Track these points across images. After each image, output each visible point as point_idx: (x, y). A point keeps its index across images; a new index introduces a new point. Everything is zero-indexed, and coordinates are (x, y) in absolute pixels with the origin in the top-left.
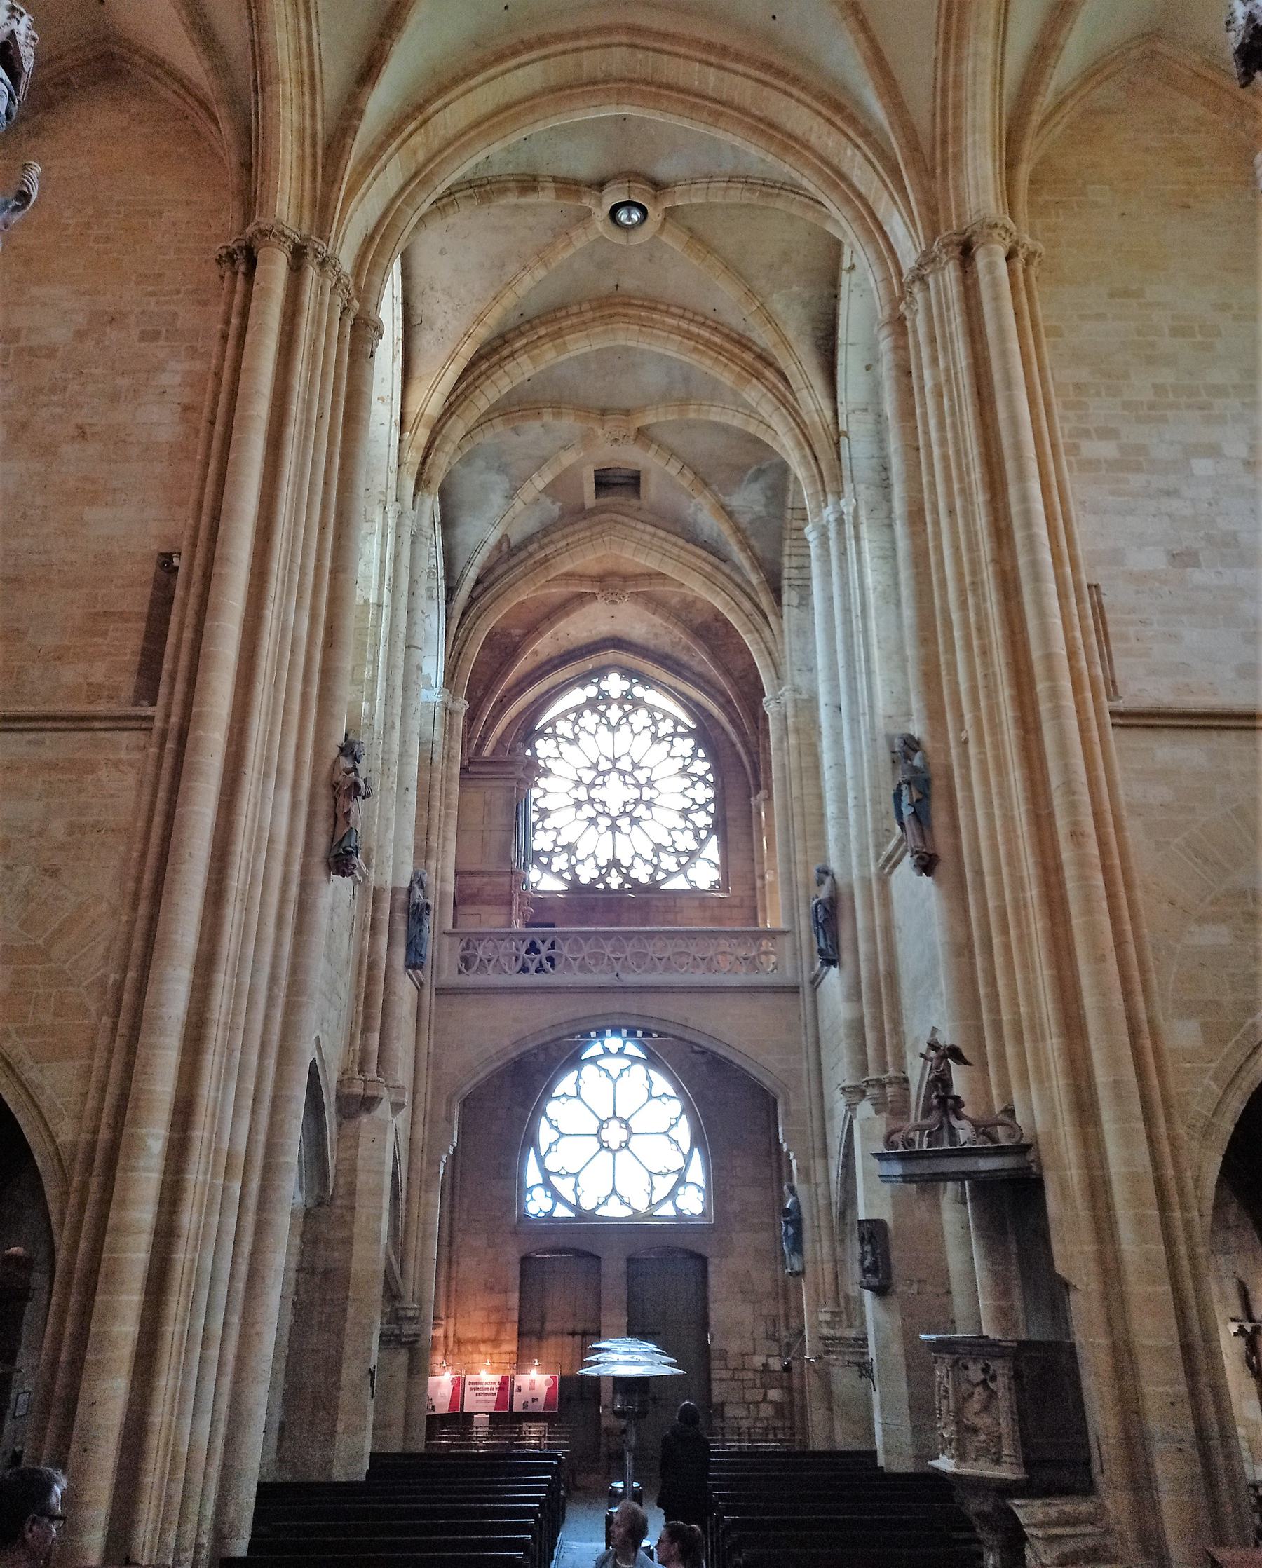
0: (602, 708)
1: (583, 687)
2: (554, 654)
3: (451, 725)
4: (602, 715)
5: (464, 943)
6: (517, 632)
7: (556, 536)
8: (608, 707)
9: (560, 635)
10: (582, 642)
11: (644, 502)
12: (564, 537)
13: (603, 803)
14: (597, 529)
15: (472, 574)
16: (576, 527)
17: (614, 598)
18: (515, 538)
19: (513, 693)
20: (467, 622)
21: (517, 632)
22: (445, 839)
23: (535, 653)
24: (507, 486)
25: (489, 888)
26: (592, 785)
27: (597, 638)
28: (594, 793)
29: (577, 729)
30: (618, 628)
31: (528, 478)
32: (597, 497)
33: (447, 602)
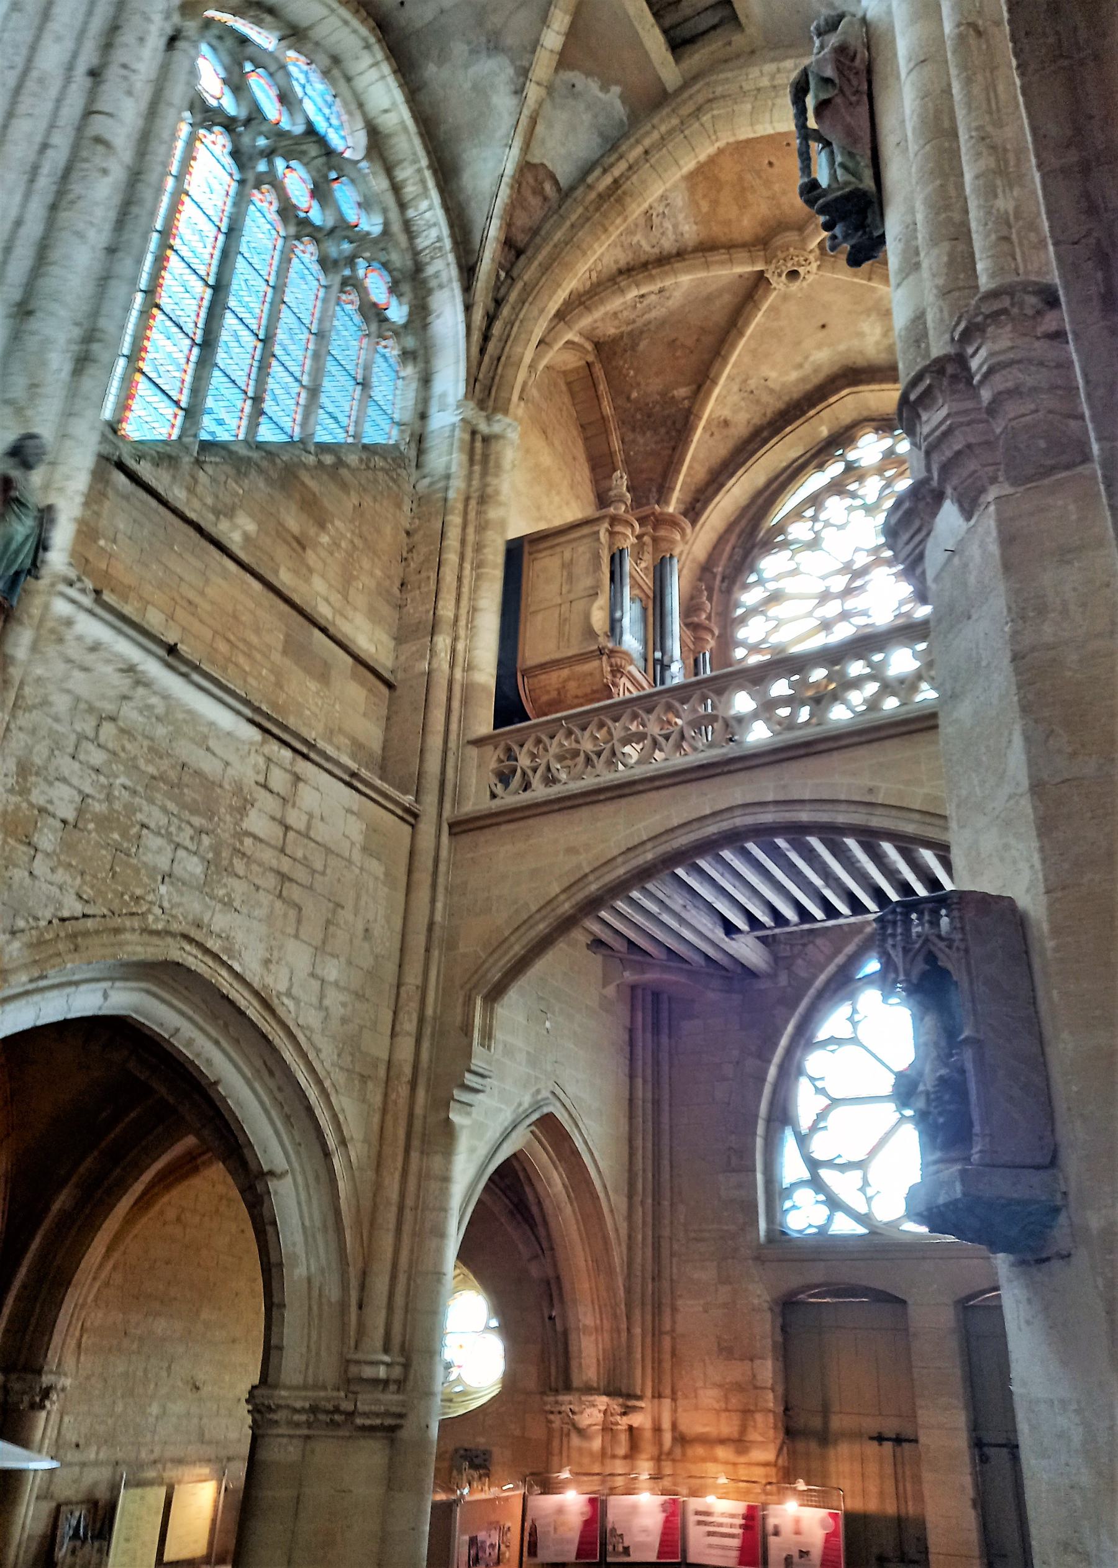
0: (852, 487)
1: (821, 467)
2: (757, 421)
3: (485, 458)
4: (853, 495)
5: (500, 753)
6: (681, 392)
7: (624, 148)
8: (861, 479)
9: (752, 383)
10: (795, 396)
11: (751, 30)
12: (638, 142)
13: (864, 613)
14: (685, 111)
15: (494, 230)
16: (655, 121)
17: (790, 267)
18: (564, 172)
19: (710, 490)
20: (506, 311)
21: (681, 392)
22: (474, 610)
23: (726, 423)
24: (511, 71)
25: (572, 685)
26: (848, 592)
27: (816, 380)
28: (851, 604)
29: (818, 526)
30: (842, 347)
31: (535, 45)
32: (677, 60)
33: (467, 288)
